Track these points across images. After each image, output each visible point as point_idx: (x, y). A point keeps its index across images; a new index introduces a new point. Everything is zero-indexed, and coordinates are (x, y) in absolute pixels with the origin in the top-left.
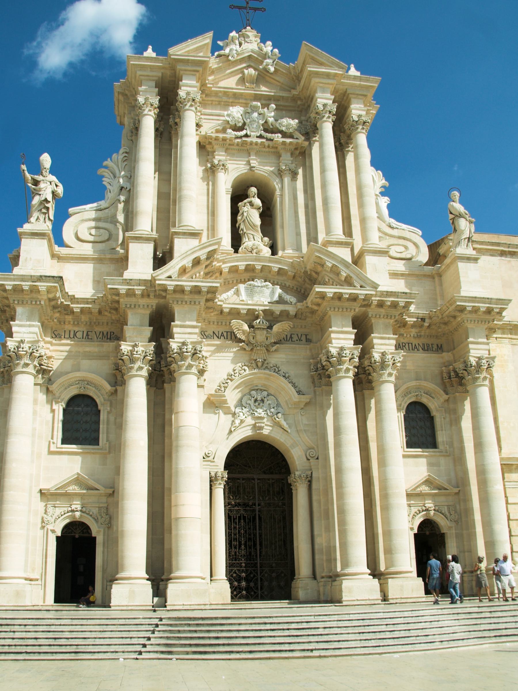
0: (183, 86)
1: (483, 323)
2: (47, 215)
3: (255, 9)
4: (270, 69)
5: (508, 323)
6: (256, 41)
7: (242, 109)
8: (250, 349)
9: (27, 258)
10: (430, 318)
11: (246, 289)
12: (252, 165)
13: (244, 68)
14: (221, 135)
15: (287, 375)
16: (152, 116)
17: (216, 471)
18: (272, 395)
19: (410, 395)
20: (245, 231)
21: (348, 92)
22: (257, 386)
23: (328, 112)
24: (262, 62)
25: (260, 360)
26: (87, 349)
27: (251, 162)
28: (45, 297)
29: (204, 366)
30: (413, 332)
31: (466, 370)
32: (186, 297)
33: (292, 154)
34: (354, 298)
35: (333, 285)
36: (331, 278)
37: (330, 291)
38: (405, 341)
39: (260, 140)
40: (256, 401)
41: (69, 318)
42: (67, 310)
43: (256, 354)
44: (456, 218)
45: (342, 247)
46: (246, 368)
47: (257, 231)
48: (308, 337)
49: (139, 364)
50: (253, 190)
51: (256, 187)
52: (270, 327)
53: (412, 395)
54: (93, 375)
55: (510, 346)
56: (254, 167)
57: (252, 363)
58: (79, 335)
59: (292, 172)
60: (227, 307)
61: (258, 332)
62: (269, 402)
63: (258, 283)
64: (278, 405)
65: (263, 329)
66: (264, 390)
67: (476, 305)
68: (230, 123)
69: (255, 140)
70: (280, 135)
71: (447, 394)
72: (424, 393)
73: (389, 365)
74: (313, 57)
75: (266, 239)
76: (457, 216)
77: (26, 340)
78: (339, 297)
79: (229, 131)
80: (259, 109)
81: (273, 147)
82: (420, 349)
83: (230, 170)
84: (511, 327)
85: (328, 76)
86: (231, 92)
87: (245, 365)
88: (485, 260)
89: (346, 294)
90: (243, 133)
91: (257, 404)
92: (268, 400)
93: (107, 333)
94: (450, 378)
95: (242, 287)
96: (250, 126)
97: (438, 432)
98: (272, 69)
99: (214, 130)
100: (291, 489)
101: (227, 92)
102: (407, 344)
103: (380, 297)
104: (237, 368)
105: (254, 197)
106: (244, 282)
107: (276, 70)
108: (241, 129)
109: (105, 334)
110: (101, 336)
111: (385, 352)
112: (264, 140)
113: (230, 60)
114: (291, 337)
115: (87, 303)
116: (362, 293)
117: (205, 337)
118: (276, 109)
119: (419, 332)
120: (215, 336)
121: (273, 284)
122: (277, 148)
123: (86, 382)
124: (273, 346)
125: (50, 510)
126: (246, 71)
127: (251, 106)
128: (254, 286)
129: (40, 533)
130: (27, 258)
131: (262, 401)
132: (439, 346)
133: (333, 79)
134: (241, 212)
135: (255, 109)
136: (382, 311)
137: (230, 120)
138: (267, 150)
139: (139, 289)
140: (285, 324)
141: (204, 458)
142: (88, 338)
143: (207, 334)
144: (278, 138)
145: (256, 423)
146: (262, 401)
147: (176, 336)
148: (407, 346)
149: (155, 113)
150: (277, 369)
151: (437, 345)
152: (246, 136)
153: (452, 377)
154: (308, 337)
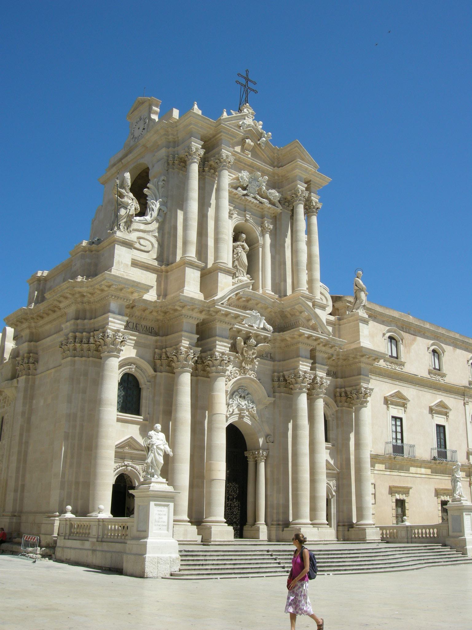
6: (252, 118)
21: (311, 182)
22: (242, 386)
27: (247, 215)
32: (227, 319)
37: (307, 332)
39: (255, 201)
46: (238, 373)
47: (245, 269)
50: (244, 236)
54: (143, 361)
71: (338, 407)
76: (360, 289)
78: (309, 337)
79: (240, 189)
88: (371, 323)
90: (245, 192)
93: (149, 327)
94: (341, 396)
97: (331, 431)
100: (247, 461)
105: (243, 242)
109: (148, 328)
111: (323, 377)
121: (262, 315)
130: (119, 261)
142: (136, 329)
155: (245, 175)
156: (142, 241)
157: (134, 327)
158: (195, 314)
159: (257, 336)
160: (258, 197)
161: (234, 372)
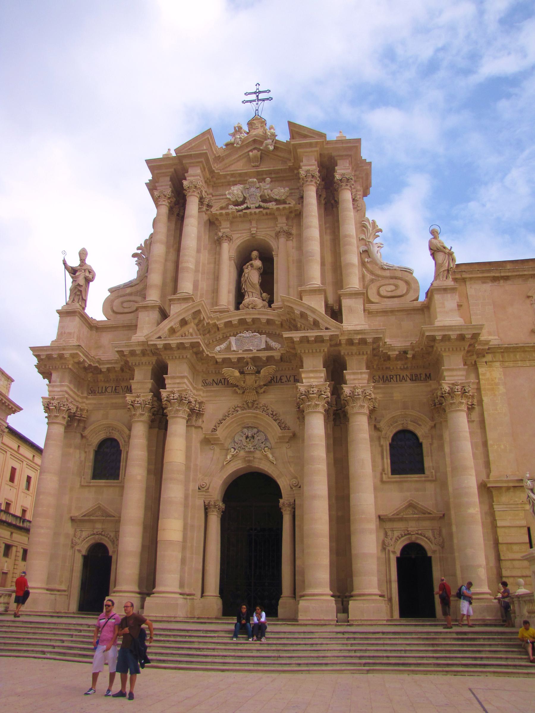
0: (189, 176)
2: (81, 297)
3: (263, 100)
4: (269, 148)
7: (242, 186)
8: (241, 392)
9: (62, 332)
10: (413, 349)
11: (237, 340)
12: (252, 232)
13: (249, 151)
14: (224, 212)
15: (274, 413)
16: (166, 205)
17: (210, 499)
18: (261, 431)
19: (395, 424)
20: (246, 289)
22: (248, 424)
23: (311, 177)
24: (262, 143)
25: (250, 401)
26: (114, 401)
28: (71, 362)
29: (201, 410)
31: (443, 397)
32: (175, 352)
33: (287, 219)
34: (319, 340)
35: (304, 329)
36: (303, 324)
39: (257, 210)
40: (247, 437)
41: (101, 377)
42: (96, 371)
43: (246, 397)
44: (435, 253)
46: (238, 409)
48: (296, 378)
49: (139, 411)
50: (255, 253)
51: (258, 251)
52: (258, 372)
53: (398, 423)
56: (254, 234)
57: (243, 405)
58: (109, 390)
59: (287, 233)
60: (220, 357)
61: (247, 377)
62: (259, 438)
63: (246, 334)
64: (267, 439)
65: (252, 374)
66: (255, 428)
67: (447, 333)
69: (253, 211)
70: (274, 203)
72: (411, 421)
73: (360, 398)
74: (297, 132)
75: (264, 295)
76: (435, 251)
77: (56, 397)
78: (305, 340)
79: (231, 207)
80: (256, 184)
81: (270, 214)
82: (408, 379)
83: (234, 239)
85: (310, 145)
86: (237, 173)
87: (238, 407)
90: (245, 206)
91: (248, 440)
92: (257, 436)
95: (233, 339)
96: (250, 199)
98: (271, 148)
99: (218, 208)
101: (234, 174)
104: (230, 409)
105: (256, 259)
106: (235, 335)
107: (276, 148)
108: (243, 203)
110: (126, 389)
112: (262, 210)
113: (236, 147)
114: (281, 379)
115: (111, 363)
116: (326, 334)
117: (206, 385)
118: (271, 181)
119: (406, 364)
120: (214, 384)
122: (274, 214)
123: (111, 428)
124: (261, 388)
125: (78, 534)
126: (251, 153)
127: (249, 182)
128: (244, 337)
129: (70, 552)
131: (253, 437)
132: (428, 375)
133: (316, 147)
134: (243, 274)
135: (252, 184)
136: (354, 349)
137: (230, 197)
139: (138, 349)
140: (269, 368)
141: (199, 489)
142: (116, 392)
143: (207, 381)
144: (272, 205)
145: (246, 457)
146: (253, 437)
147: (167, 386)
148: (395, 378)
149: (168, 202)
150: (266, 408)
151: (426, 375)
152: (247, 208)
153: (436, 404)
154: (296, 378)
155: (236, 191)
156: (125, 305)
157: (113, 389)
158: (144, 359)
159: (255, 359)
160: (262, 204)
161: (233, 410)
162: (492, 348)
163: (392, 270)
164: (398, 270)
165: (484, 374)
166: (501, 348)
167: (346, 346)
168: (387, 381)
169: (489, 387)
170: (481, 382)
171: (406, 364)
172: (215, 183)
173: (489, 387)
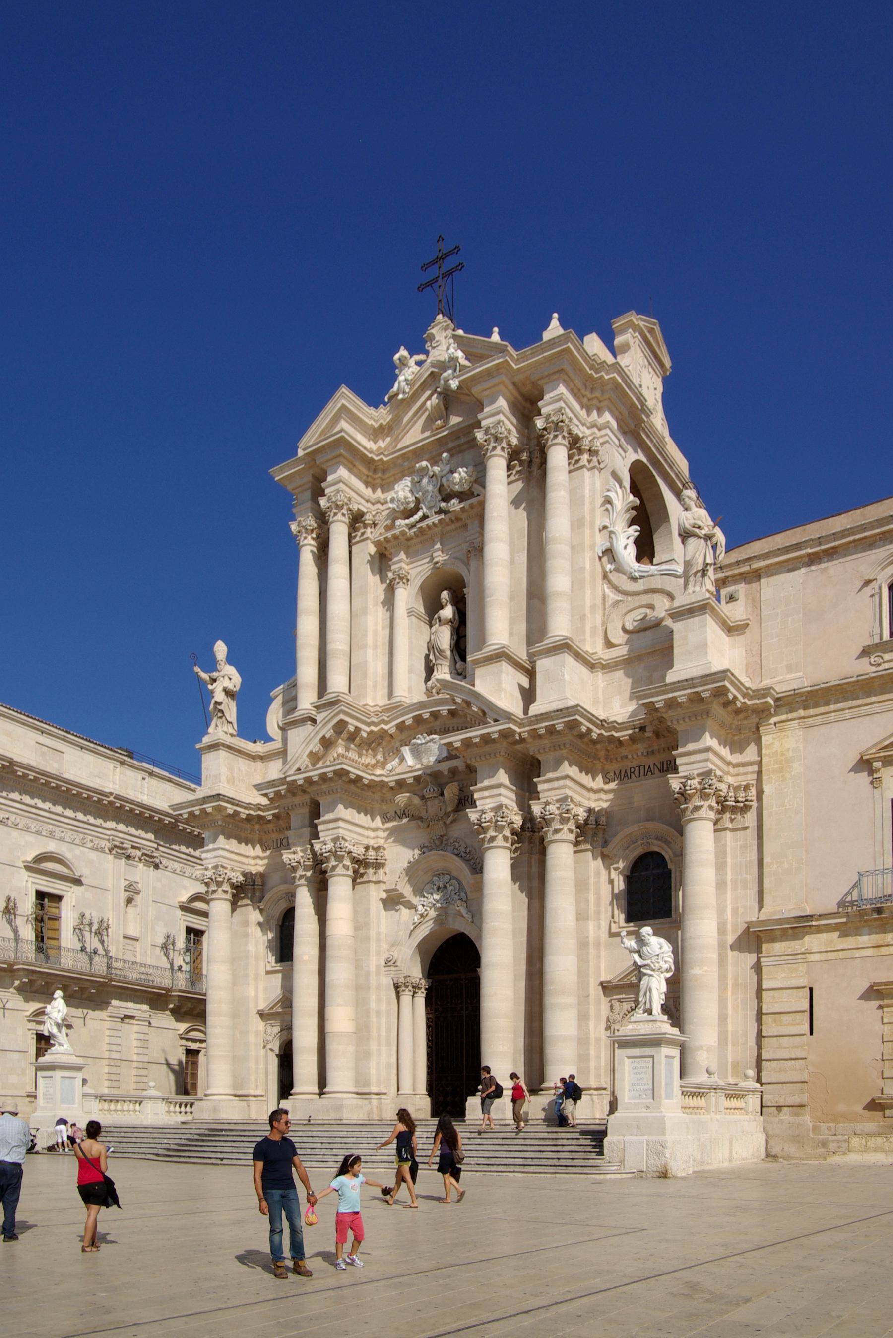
1: (699, 718)
5: (792, 692)
29: (378, 858)
30: (641, 747)
38: (634, 764)
45: (492, 663)
55: (800, 733)
68: (398, 510)
79: (399, 522)
84: (804, 698)
89: (475, 737)
102: (637, 769)
103: (529, 725)
136: (546, 742)
138: (453, 527)
152: (425, 517)
162: (783, 697)
163: (648, 576)
164: (657, 575)
165: (769, 746)
166: (801, 694)
167: (534, 740)
168: (626, 779)
169: (776, 767)
170: (763, 761)
171: (650, 747)
172: (383, 480)
173: (776, 767)
